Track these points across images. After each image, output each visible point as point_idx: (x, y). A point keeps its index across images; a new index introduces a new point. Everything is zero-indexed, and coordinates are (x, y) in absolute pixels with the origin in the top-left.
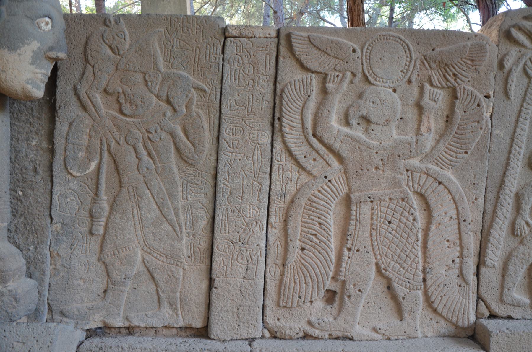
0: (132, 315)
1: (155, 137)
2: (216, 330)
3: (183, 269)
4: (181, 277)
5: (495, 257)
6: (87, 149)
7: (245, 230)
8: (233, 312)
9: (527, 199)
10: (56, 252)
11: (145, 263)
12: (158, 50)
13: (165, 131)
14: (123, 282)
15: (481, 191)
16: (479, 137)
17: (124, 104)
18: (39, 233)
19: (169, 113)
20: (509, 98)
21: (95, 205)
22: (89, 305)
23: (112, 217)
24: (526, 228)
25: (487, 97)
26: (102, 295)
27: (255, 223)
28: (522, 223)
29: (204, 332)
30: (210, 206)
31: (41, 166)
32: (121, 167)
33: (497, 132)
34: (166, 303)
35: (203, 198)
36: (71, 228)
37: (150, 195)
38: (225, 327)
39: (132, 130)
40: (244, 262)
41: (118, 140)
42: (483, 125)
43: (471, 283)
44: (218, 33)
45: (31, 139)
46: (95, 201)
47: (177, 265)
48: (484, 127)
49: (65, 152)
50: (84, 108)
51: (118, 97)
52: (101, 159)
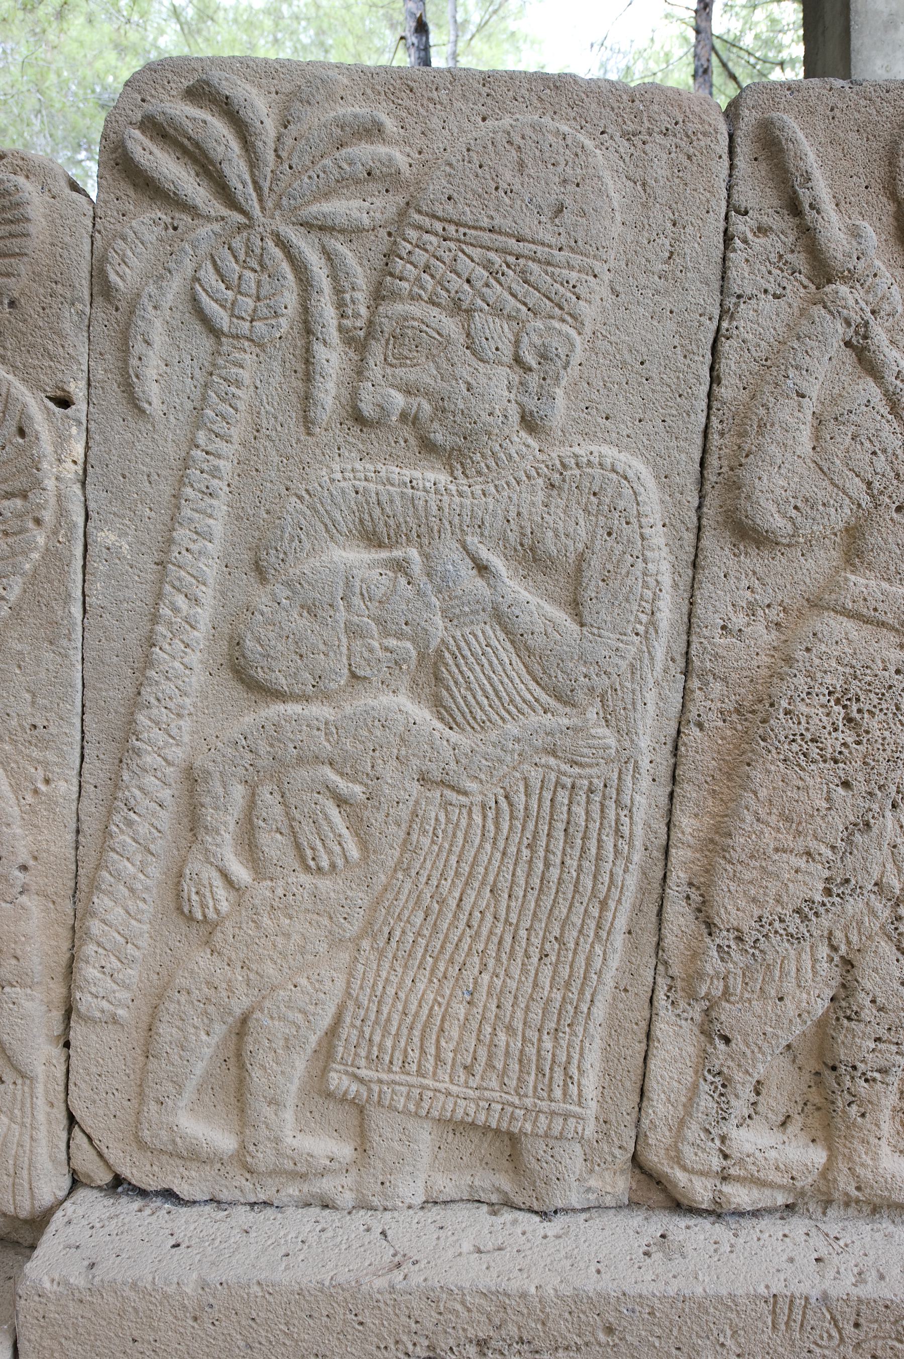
5: (108, 987)
9: (220, 791)
15: (62, 755)
16: (35, 556)
20: (142, 411)
24: (221, 892)
25: (64, 402)
28: (204, 875)
33: (105, 537)
42: (40, 507)
43: (40, 1070)
48: (48, 516)
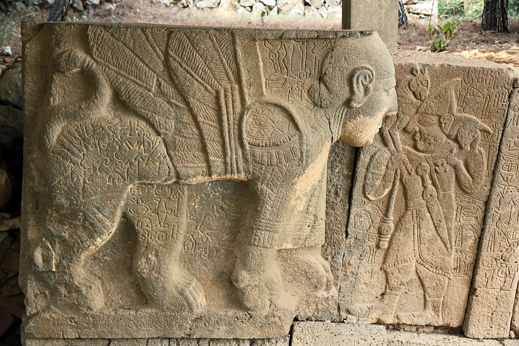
0: (401, 314)
1: (440, 170)
2: (472, 330)
3: (449, 278)
4: (446, 285)
6: (383, 178)
7: (507, 250)
8: (488, 316)
10: (348, 261)
11: (417, 273)
12: (454, 97)
13: (450, 165)
14: (399, 288)
17: (419, 142)
18: (336, 246)
19: (455, 150)
21: (384, 224)
22: (369, 305)
23: (397, 234)
26: (380, 297)
27: (516, 244)
29: (460, 331)
30: (478, 228)
31: (342, 189)
32: (409, 193)
34: (430, 306)
35: (473, 221)
36: (362, 242)
37: (429, 217)
38: (480, 328)
39: (423, 164)
40: (503, 276)
41: (410, 171)
44: (508, 83)
45: (335, 167)
46: (383, 221)
47: (444, 275)
49: (365, 180)
50: (386, 145)
51: (415, 135)
52: (394, 186)
